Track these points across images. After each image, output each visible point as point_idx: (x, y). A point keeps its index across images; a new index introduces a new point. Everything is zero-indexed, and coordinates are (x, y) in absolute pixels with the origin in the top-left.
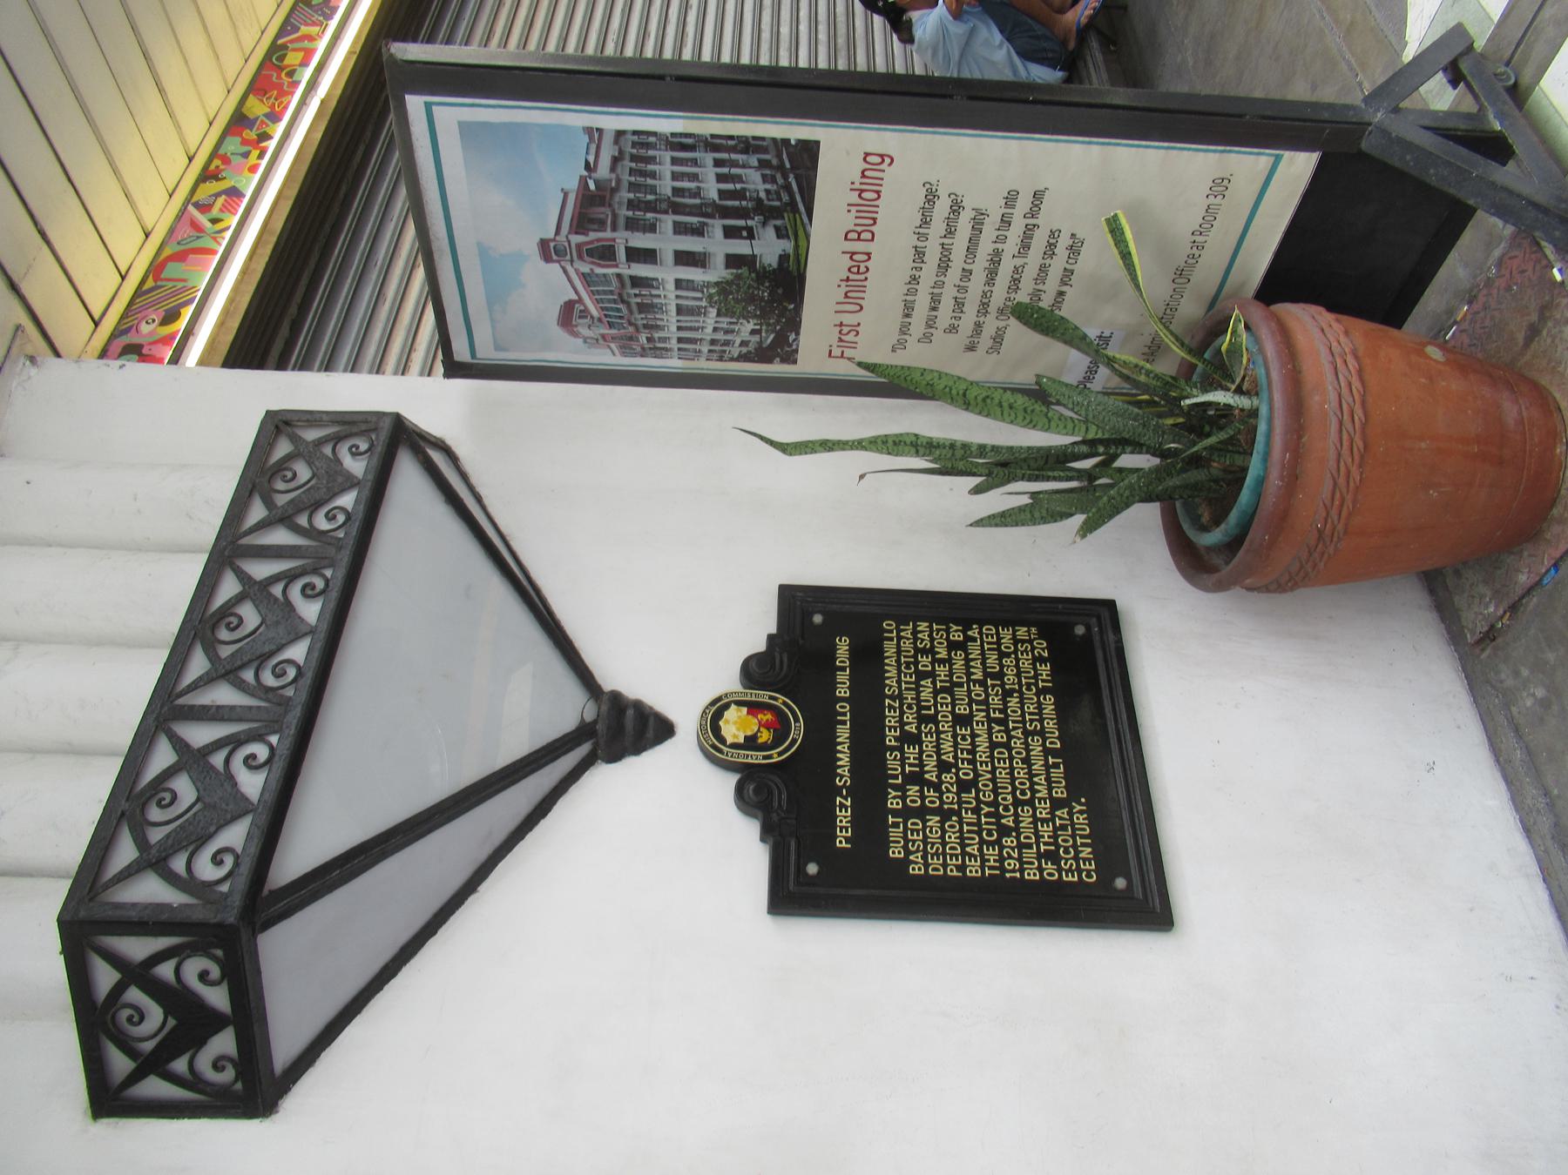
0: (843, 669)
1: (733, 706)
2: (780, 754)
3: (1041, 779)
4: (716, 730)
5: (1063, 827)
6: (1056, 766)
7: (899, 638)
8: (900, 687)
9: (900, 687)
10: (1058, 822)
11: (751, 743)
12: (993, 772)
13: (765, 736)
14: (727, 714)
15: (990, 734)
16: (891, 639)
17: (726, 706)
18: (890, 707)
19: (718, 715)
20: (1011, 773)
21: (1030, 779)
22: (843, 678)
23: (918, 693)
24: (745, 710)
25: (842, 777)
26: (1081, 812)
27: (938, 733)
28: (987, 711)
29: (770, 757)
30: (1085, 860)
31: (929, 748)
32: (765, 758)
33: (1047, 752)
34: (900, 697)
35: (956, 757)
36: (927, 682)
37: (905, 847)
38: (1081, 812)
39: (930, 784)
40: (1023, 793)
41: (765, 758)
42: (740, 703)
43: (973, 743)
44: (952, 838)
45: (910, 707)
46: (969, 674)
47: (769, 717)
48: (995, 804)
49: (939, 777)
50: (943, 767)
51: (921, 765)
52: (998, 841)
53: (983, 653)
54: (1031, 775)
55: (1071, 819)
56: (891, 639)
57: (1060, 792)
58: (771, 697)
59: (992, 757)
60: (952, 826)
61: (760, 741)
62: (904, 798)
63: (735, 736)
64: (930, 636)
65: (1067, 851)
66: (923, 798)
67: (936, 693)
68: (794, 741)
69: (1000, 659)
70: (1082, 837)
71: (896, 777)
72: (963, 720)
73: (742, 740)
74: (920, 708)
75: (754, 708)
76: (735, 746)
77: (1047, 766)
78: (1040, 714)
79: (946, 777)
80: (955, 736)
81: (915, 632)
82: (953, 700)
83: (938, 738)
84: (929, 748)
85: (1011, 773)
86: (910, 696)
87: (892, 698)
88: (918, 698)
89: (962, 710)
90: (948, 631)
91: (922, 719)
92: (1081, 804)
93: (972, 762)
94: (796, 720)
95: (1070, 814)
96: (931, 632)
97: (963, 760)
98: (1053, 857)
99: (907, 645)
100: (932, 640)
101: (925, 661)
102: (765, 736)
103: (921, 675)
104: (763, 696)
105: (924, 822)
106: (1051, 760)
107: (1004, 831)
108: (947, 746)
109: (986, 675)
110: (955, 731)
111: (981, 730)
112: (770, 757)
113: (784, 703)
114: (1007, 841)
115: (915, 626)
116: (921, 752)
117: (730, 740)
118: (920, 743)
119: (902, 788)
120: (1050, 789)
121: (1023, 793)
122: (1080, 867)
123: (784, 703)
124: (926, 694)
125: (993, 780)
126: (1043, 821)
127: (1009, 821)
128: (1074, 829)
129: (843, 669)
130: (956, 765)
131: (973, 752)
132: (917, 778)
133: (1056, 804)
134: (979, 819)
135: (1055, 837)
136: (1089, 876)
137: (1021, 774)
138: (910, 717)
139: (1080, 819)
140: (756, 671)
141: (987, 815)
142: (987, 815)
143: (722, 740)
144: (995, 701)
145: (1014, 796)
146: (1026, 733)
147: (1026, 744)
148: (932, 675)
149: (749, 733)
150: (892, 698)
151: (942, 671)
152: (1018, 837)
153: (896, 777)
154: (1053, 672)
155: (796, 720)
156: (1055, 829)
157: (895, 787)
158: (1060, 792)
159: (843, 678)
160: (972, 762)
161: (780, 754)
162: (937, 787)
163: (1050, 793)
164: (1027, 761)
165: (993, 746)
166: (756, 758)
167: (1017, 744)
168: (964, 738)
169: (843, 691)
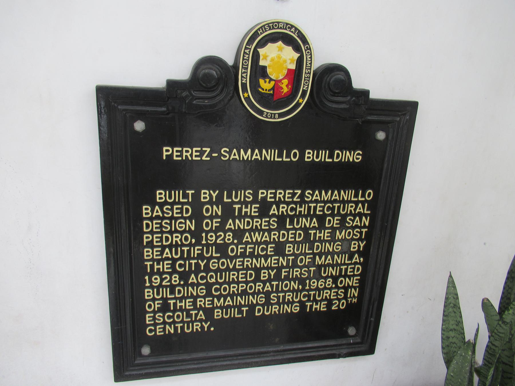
0: (331, 156)
1: (296, 55)
2: (248, 99)
3: (229, 302)
4: (273, 38)
5: (189, 315)
6: (240, 312)
7: (357, 203)
8: (311, 202)
9: (311, 202)
10: (193, 312)
11: (259, 72)
12: (234, 269)
13: (265, 86)
15: (268, 268)
16: (356, 196)
17: (297, 49)
18: (294, 194)
19: (288, 40)
20: (233, 282)
21: (229, 294)
22: (323, 156)
23: (306, 217)
24: (293, 67)
25: (230, 153)
26: (202, 327)
27: (270, 231)
28: (287, 266)
29: (245, 90)
30: (164, 329)
31: (257, 223)
32: (244, 85)
33: (252, 307)
34: (302, 201)
35: (247, 243)
36: (315, 223)
37: (166, 203)
38: (202, 327)
39: (223, 223)
40: (216, 290)
41: (244, 85)
42: (300, 62)
43: (258, 257)
44: (176, 238)
45: (292, 209)
46: (320, 255)
48: (207, 269)
49: (230, 230)
50: (239, 234)
51: (241, 217)
52: (175, 271)
53: (337, 265)
54: (232, 296)
55: (196, 321)
56: (356, 196)
57: (218, 314)
59: (248, 269)
60: (186, 239)
62: (211, 202)
63: (265, 58)
64: (356, 227)
65: (169, 317)
66: (211, 218)
67: (306, 230)
68: (261, 113)
69: (332, 276)
70: (182, 328)
71: (229, 196)
72: (280, 249)
73: (262, 63)
74: (292, 218)
75: (295, 76)
76: (256, 56)
77: (241, 305)
78: (284, 302)
79: (229, 236)
80: (266, 243)
81: (360, 215)
82: (298, 243)
83: (264, 231)
84: (257, 223)
85: (233, 282)
86: (303, 209)
87: (302, 196)
88: (300, 215)
89: (289, 249)
90: (360, 239)
91: (281, 219)
92: (209, 328)
93: (243, 255)
94: (281, 115)
95: (201, 321)
96: (360, 227)
97: (245, 249)
98: (165, 308)
99: (350, 208)
100: (353, 228)
101: (335, 222)
102: (265, 86)
103: (321, 219)
104: (306, 84)
105: (190, 218)
106: (245, 309)
107: (184, 276)
108: (257, 237)
109: (319, 267)
110: (270, 243)
111: (272, 262)
112: (245, 90)
113: (298, 105)
114: (176, 279)
115: (366, 215)
116: (252, 218)
117: (261, 51)
118: (261, 217)
119: (219, 201)
120: (221, 308)
121: (216, 290)
122: (156, 324)
123: (298, 105)
124: (305, 222)
125: (228, 269)
126: (194, 303)
127: (193, 279)
128: (188, 323)
129: (331, 156)
130: (240, 242)
131: (252, 255)
132: (228, 212)
133: (209, 312)
134: (194, 258)
135: (181, 310)
136: (151, 331)
137: (234, 288)
138: (283, 208)
139: (197, 326)
140: (334, 79)
141: (197, 265)
142: (197, 265)
143: (263, 43)
144: (296, 272)
145: (214, 284)
146: (267, 295)
147: (259, 292)
148: (321, 226)
149: (269, 71)
150: (302, 196)
151: (325, 234)
152: (179, 285)
153: (229, 196)
154: (318, 313)
155: (281, 115)
156: (188, 311)
157: (220, 197)
158: (218, 314)
159: (323, 156)
160: (243, 255)
161: (248, 99)
162: (222, 228)
163: (217, 307)
164: (244, 293)
165: (258, 271)
166: (244, 77)
167: (259, 286)
168: (263, 250)
169: (310, 155)
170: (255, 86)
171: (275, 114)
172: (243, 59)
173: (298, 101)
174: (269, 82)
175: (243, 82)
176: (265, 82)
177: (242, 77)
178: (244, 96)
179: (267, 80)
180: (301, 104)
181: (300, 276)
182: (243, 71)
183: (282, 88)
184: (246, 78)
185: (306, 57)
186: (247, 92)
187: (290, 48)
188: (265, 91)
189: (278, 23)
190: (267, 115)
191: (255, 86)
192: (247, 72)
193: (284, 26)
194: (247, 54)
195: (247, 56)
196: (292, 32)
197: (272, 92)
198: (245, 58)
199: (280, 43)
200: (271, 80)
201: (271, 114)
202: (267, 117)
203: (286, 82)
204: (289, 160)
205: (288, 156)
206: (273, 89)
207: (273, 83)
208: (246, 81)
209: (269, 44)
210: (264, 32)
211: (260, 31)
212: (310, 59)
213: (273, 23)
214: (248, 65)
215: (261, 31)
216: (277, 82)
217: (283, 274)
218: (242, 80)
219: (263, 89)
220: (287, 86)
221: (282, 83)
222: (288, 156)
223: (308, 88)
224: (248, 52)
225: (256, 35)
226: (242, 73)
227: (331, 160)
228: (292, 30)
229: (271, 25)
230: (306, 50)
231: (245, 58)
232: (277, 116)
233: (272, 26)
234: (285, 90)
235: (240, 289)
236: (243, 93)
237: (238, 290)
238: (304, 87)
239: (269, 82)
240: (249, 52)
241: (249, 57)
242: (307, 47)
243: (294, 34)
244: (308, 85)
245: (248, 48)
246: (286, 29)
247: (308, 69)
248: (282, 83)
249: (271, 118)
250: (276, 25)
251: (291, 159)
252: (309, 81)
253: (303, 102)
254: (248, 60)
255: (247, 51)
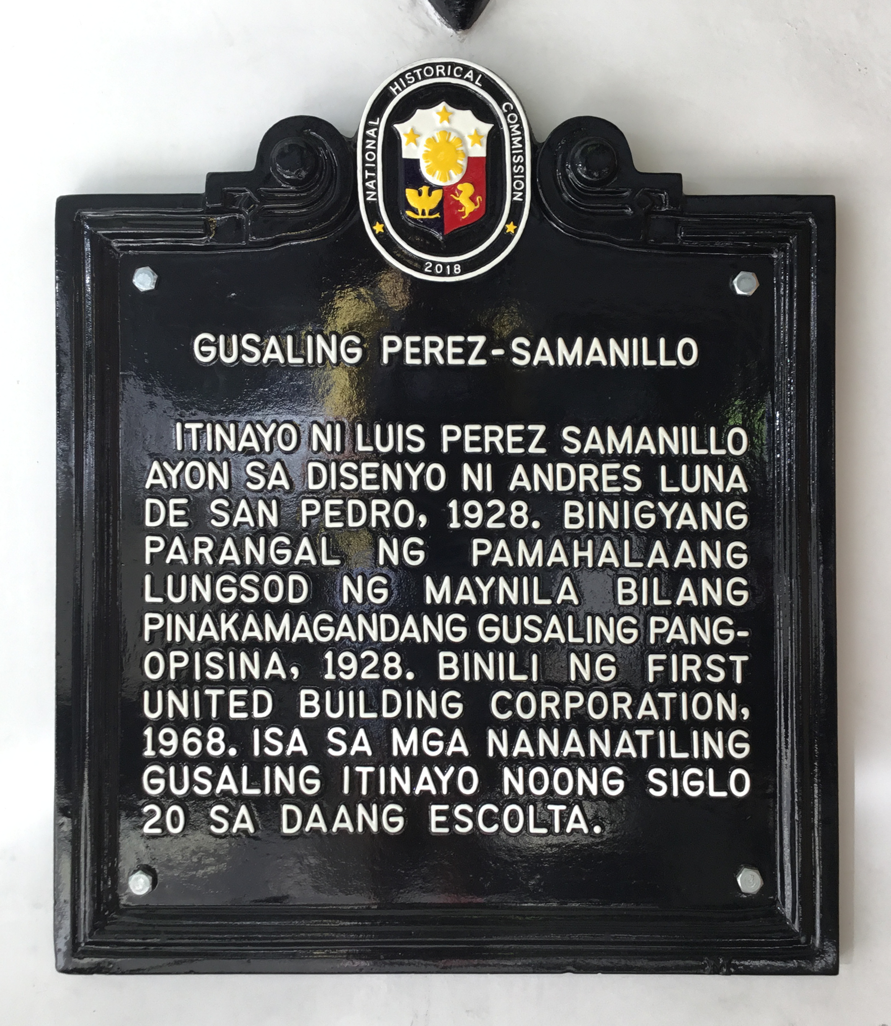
11: (404, 174)
13: (421, 203)
14: (467, 115)
17: (483, 113)
19: (460, 98)
29: (374, 217)
40: (503, 705)
42: (495, 141)
47: (468, 207)
58: (517, 207)
61: (411, 194)
75: (488, 172)
76: (392, 141)
94: (467, 266)
102: (421, 203)
112: (374, 217)
113: (505, 238)
121: (503, 705)
123: (505, 238)
143: (404, 112)
145: (497, 685)
155: (467, 266)
166: (370, 187)
170: (396, 205)
171: (452, 265)
172: (364, 151)
173: (504, 229)
174: (430, 194)
175: (368, 199)
176: (420, 194)
177: (366, 189)
178: (374, 231)
179: (425, 189)
180: (510, 237)
181: (703, 678)
182: (367, 174)
183: (459, 205)
184: (376, 190)
185: (510, 129)
186: (381, 222)
187: (468, 114)
188: (420, 217)
189: (433, 65)
190: (432, 268)
191: (396, 205)
192: (375, 178)
193: (446, 71)
194: (372, 138)
195: (374, 142)
196: (468, 80)
197: (437, 215)
198: (368, 147)
199: (443, 104)
200: (432, 188)
201: (444, 265)
202: (433, 274)
203: (467, 189)
204: (673, 363)
205: (671, 354)
206: (440, 208)
207: (437, 195)
208: (376, 196)
209: (419, 111)
210: (403, 89)
211: (394, 86)
212: (519, 133)
213: (423, 67)
214: (375, 162)
215: (398, 87)
216: (448, 191)
217: (652, 669)
218: (365, 196)
219: (415, 211)
220: (472, 199)
221: (460, 192)
222: (671, 354)
223: (523, 197)
224: (373, 135)
225: (385, 97)
226: (365, 181)
227: (653, 363)
228: (467, 75)
229: (418, 71)
230: (505, 115)
231: (368, 147)
232: (457, 268)
233: (421, 73)
234: (468, 207)
235: (569, 706)
236: (372, 224)
237: (561, 708)
238: (513, 196)
239: (430, 194)
240: (377, 133)
241: (375, 145)
242: (507, 107)
243: (473, 82)
244: (524, 189)
245: (372, 127)
246: (452, 76)
247: (517, 155)
248: (460, 192)
249: (443, 274)
250: (428, 72)
251: (678, 361)
252: (524, 180)
253: (516, 231)
254: (375, 151)
255: (371, 132)
